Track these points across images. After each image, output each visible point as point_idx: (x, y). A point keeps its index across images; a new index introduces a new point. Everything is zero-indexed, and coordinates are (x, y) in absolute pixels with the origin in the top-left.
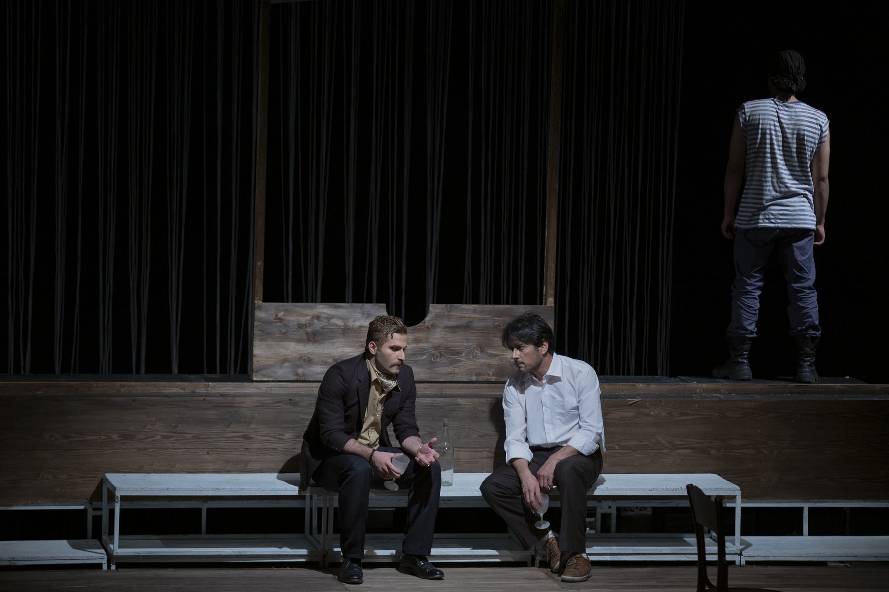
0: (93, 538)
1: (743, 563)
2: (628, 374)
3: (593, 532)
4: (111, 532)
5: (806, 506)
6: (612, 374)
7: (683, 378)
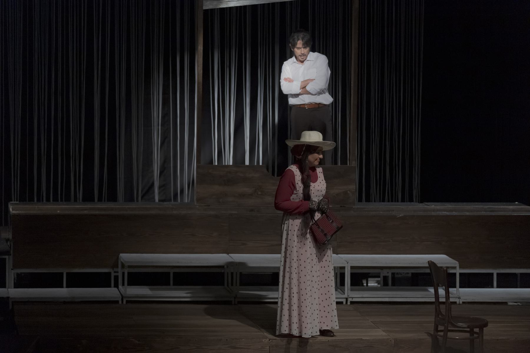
0: (115, 287)
1: (461, 302)
2: (398, 201)
3: (379, 286)
4: (123, 285)
5: (495, 272)
6: (389, 201)
7: (426, 203)
